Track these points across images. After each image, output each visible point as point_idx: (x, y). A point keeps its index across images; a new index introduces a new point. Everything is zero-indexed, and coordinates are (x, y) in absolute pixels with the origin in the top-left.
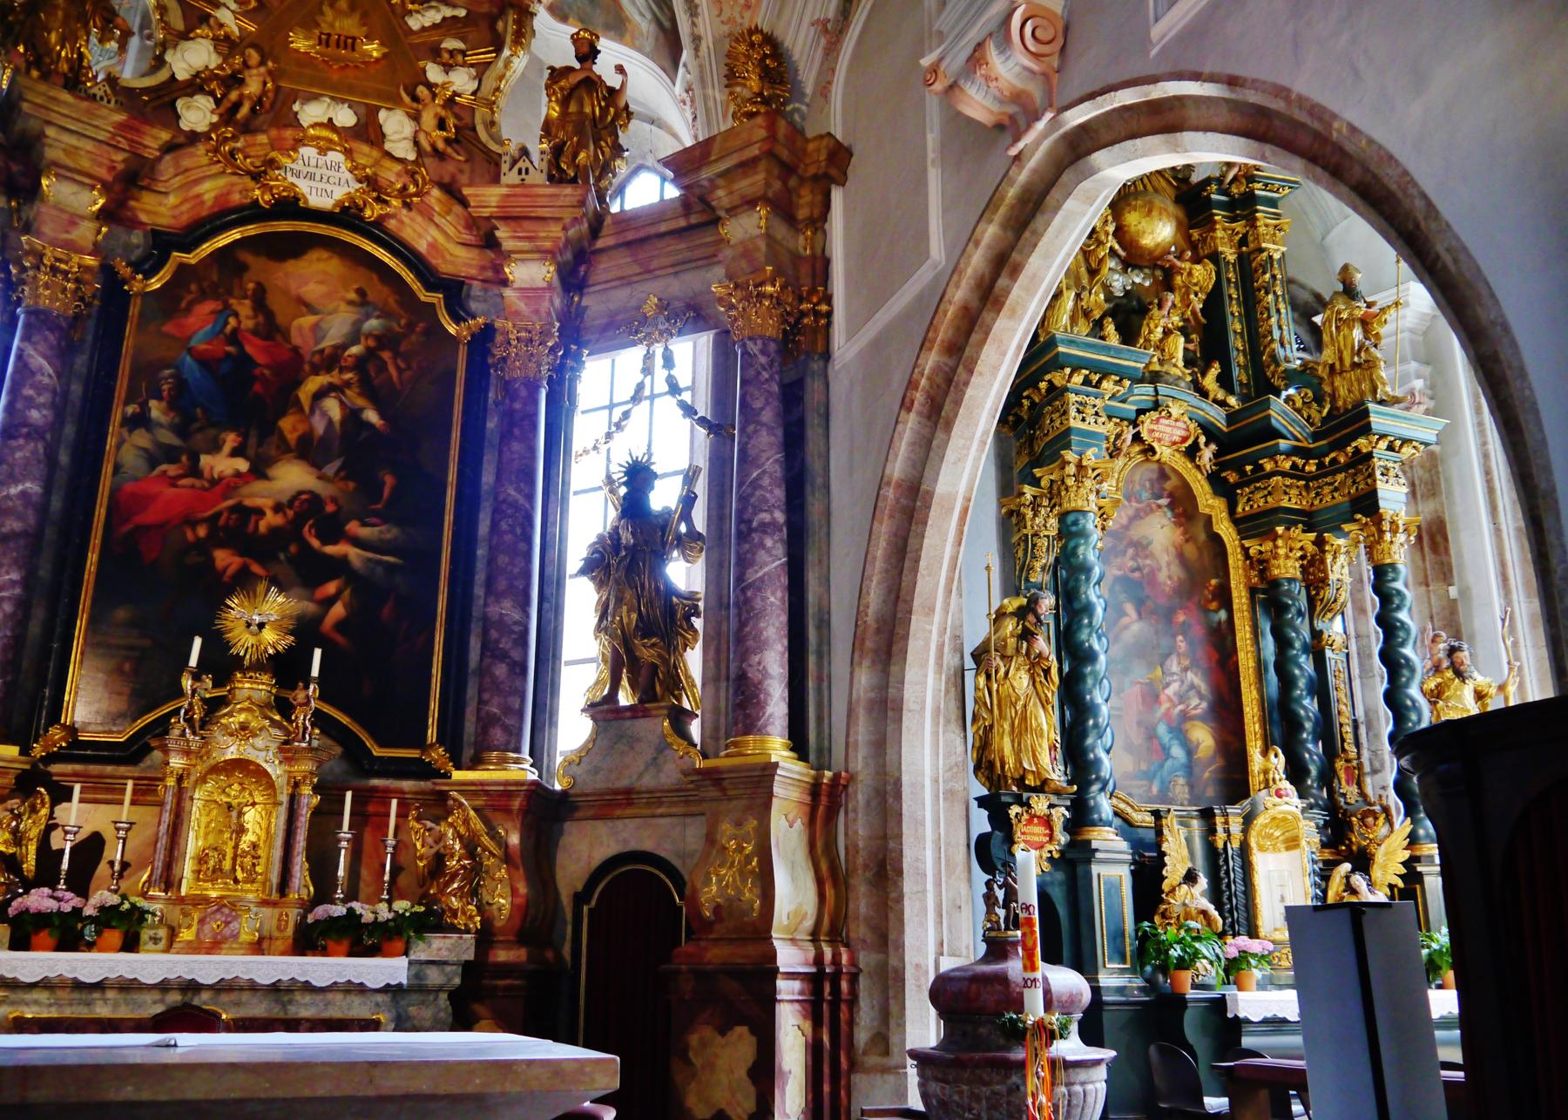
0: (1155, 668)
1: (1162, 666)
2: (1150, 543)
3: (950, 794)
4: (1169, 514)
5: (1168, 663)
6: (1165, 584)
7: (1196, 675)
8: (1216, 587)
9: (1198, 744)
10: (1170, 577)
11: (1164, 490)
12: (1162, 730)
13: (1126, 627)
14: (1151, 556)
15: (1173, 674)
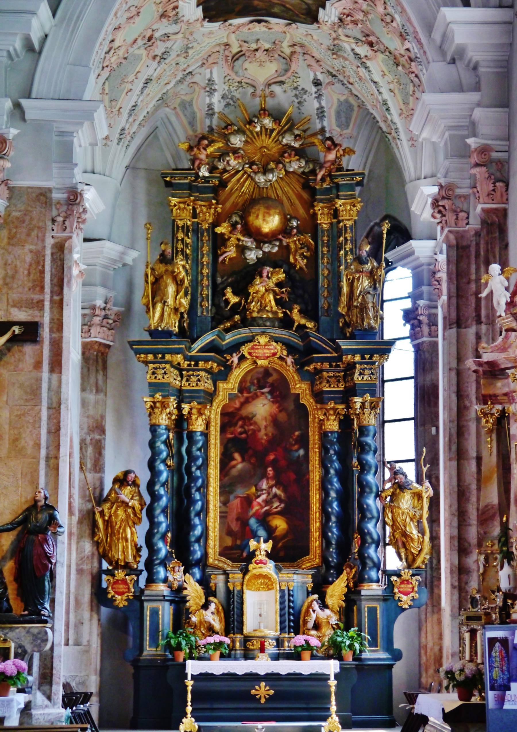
0: (250, 488)
1: (256, 486)
2: (254, 416)
3: (80, 572)
4: (269, 397)
5: (260, 483)
6: (262, 439)
7: (279, 489)
8: (298, 436)
9: (276, 528)
10: (266, 435)
11: (268, 383)
12: (253, 522)
13: (234, 466)
14: (255, 423)
15: (263, 490)
